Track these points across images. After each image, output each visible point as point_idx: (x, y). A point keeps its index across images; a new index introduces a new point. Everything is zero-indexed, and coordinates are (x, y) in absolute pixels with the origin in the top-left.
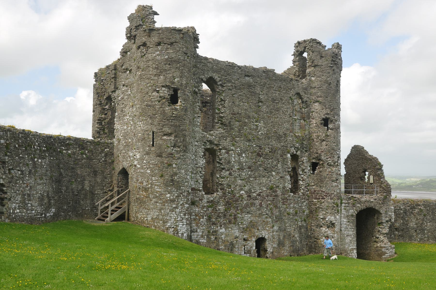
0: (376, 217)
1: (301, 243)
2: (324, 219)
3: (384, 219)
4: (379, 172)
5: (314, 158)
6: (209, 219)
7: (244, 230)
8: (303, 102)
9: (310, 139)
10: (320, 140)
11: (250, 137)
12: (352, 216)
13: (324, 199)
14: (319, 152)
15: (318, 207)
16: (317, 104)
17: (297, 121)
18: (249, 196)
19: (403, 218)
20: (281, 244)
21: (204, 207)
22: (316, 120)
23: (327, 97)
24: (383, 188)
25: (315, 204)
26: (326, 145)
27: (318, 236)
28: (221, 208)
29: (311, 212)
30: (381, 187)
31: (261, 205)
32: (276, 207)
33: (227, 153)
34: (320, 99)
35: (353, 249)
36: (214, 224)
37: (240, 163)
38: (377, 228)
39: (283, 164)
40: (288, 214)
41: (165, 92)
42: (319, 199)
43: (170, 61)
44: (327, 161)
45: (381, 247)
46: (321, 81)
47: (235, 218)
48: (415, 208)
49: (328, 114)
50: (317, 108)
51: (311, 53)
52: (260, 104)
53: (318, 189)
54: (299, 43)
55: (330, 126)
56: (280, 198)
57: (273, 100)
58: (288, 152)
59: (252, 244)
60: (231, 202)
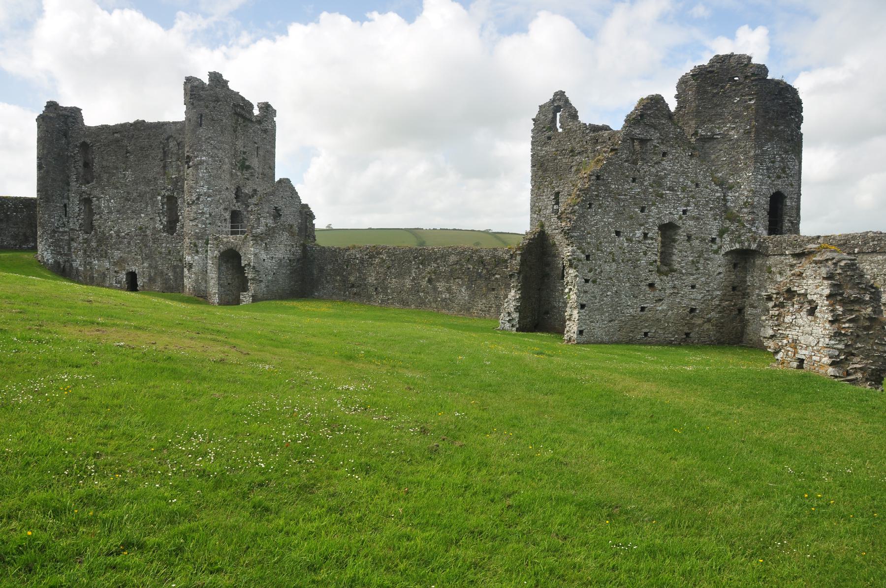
1: (176, 280)
6: (85, 251)
7: (115, 264)
11: (118, 185)
17: (173, 163)
18: (118, 235)
19: (359, 271)
20: (152, 280)
21: (80, 243)
28: (94, 244)
31: (129, 243)
32: (146, 246)
33: (98, 200)
36: (89, 256)
37: (109, 207)
39: (152, 206)
40: (161, 253)
47: (106, 253)
48: (375, 257)
56: (150, 238)
57: (142, 148)
58: (159, 195)
59: (123, 276)
60: (103, 240)
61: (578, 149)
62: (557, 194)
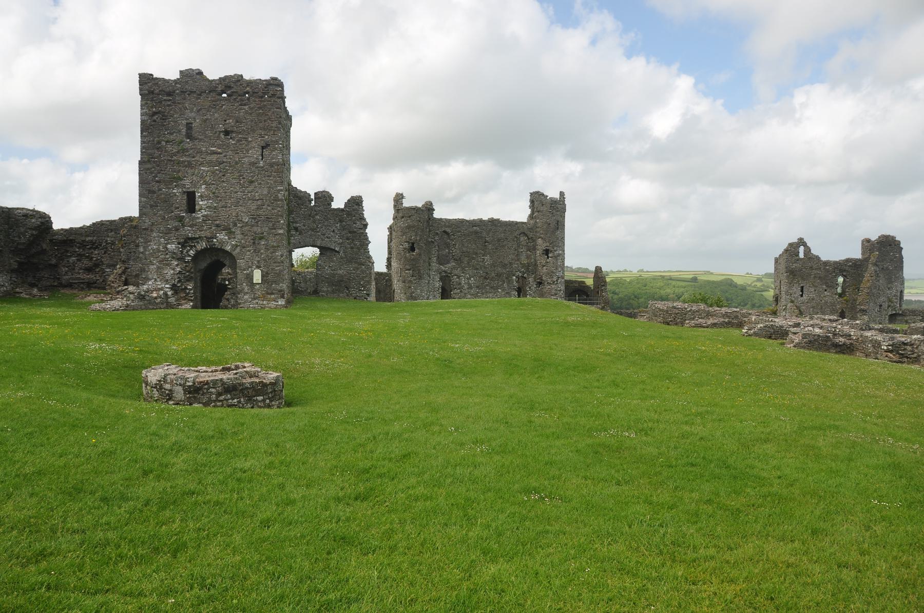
9: (536, 265)
37: (469, 284)
41: (406, 245)
43: (409, 227)
55: (550, 255)
57: (499, 240)
61: (815, 267)
62: (802, 287)
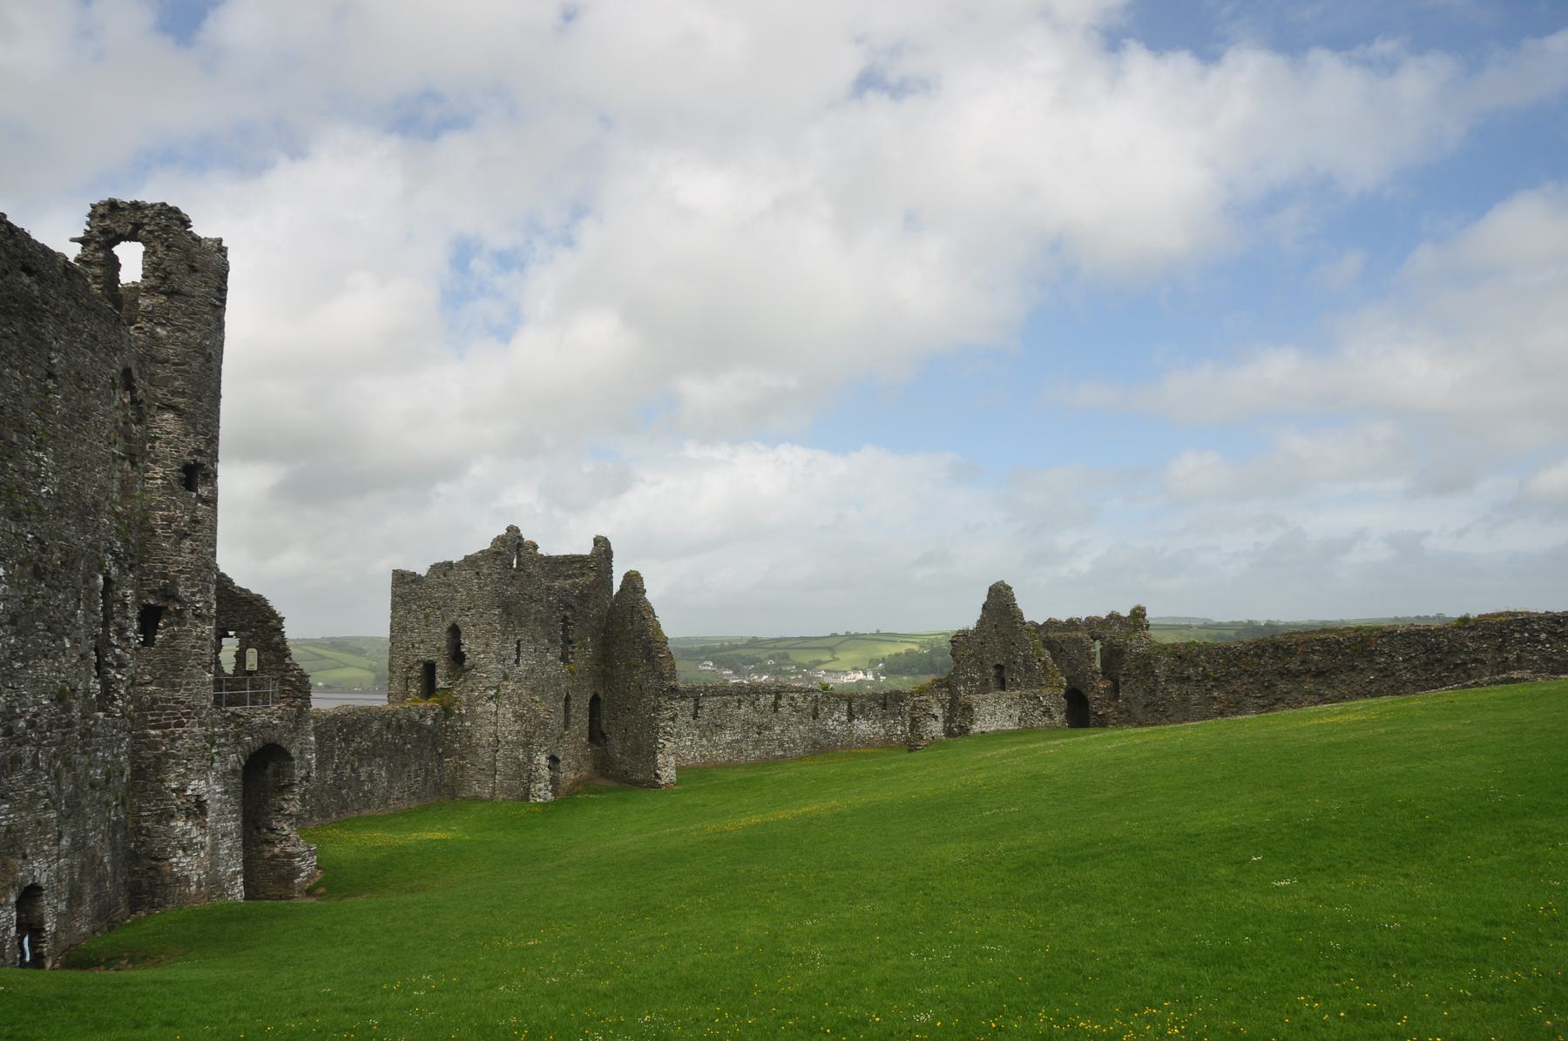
0: (269, 771)
2: (181, 790)
3: (299, 773)
4: (276, 639)
5: (152, 592)
8: (133, 401)
10: (175, 532)
12: (234, 771)
13: (181, 725)
14: (172, 570)
15: (166, 754)
16: (168, 416)
22: (165, 466)
23: (199, 399)
24: (291, 684)
25: (154, 745)
26: (192, 552)
27: (163, 850)
29: (138, 773)
30: (283, 681)
34: (180, 401)
35: (235, 873)
38: (275, 800)
42: (168, 726)
44: (193, 602)
45: (291, 856)
46: (185, 344)
49: (199, 452)
50: (169, 427)
51: (160, 249)
52: (51, 384)
53: (167, 694)
54: (113, 206)
